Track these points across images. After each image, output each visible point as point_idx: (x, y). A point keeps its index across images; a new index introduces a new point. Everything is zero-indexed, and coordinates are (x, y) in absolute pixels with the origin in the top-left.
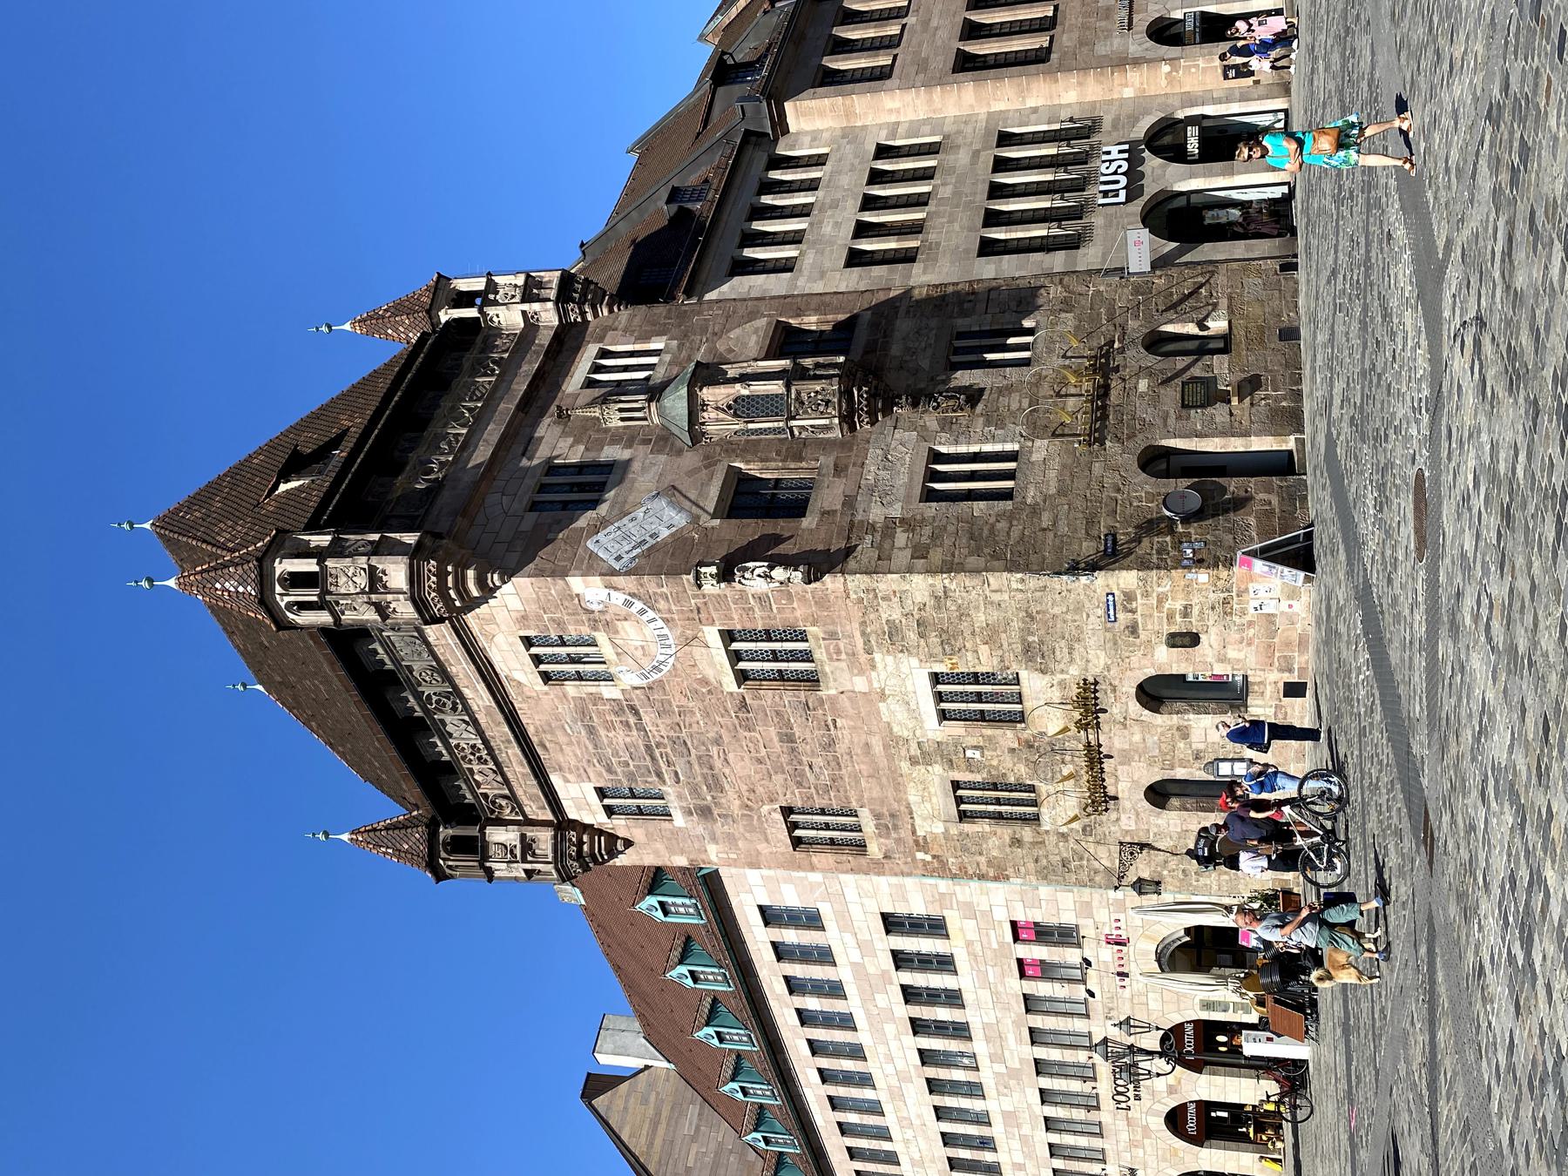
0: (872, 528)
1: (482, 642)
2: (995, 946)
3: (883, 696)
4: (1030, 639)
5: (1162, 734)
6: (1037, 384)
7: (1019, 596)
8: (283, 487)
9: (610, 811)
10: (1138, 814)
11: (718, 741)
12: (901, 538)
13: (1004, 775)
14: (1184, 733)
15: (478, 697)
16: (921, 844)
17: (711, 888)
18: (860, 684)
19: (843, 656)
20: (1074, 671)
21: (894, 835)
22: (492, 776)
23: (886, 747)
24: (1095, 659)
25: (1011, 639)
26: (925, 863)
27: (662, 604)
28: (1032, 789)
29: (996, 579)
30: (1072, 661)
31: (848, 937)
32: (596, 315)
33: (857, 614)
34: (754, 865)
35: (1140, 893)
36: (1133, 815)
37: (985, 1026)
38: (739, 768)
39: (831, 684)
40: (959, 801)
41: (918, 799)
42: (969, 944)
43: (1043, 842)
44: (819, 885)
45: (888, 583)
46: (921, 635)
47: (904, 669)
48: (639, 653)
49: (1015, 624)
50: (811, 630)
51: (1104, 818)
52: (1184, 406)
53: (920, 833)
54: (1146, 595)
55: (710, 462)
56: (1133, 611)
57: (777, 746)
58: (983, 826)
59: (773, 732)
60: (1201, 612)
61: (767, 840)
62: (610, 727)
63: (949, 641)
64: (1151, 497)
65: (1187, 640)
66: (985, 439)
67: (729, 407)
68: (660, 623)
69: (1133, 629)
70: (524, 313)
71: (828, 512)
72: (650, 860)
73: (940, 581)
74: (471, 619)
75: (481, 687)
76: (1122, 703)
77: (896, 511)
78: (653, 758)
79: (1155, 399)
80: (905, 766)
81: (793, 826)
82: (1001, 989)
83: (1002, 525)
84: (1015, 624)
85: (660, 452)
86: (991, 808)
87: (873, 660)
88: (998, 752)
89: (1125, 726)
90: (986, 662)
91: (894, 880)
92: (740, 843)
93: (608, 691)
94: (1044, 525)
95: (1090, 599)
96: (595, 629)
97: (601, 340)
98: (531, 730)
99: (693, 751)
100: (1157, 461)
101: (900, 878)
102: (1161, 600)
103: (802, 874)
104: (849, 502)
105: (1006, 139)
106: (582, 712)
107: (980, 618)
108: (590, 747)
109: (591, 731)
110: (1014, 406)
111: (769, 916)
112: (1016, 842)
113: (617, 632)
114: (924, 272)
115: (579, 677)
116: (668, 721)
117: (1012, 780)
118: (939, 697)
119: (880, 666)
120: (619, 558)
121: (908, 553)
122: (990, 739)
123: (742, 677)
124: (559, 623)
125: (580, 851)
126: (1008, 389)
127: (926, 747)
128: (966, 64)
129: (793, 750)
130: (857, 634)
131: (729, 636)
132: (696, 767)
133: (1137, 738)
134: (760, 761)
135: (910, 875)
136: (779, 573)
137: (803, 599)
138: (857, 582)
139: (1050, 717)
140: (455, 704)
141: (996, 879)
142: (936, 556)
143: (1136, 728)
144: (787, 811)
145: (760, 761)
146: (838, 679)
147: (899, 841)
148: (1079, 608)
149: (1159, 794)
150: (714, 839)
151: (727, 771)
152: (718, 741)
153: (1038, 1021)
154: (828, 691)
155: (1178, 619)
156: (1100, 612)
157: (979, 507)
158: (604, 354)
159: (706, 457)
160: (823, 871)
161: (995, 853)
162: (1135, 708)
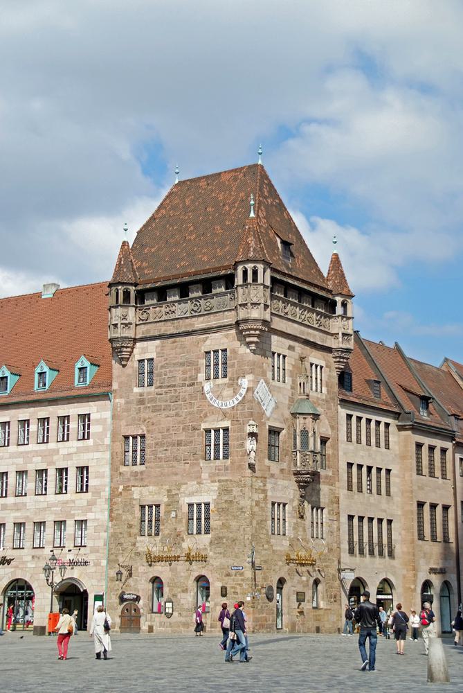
0: (265, 485)
1: (224, 333)
2: (72, 512)
3: (199, 483)
5: (184, 583)
6: (306, 541)
7: (242, 537)
8: (279, 241)
9: (141, 361)
10: (146, 573)
11: (177, 415)
12: (262, 496)
13: (164, 525)
14: (185, 591)
15: (199, 323)
17: (100, 394)
18: (205, 475)
20: (211, 554)
21: (132, 478)
22: (160, 315)
24: (216, 561)
25: (225, 533)
26: (117, 489)
28: (157, 534)
30: (215, 553)
31: (74, 450)
32: (335, 362)
33: (237, 478)
34: (114, 417)
35: (44, 569)
37: (24, 504)
38: (164, 420)
40: (150, 506)
41: (151, 491)
42: (73, 501)
43: (130, 536)
44: (103, 442)
47: (212, 493)
49: (231, 535)
51: (145, 560)
52: (297, 593)
54: (242, 580)
55: (285, 421)
56: (235, 575)
57: (175, 439)
58: (138, 514)
59: (183, 438)
61: (127, 425)
62: (184, 372)
63: (222, 511)
66: (290, 523)
67: (305, 428)
69: (228, 575)
70: (338, 334)
74: (233, 332)
75: (203, 326)
76: (197, 569)
77: (269, 493)
79: (300, 582)
80: (167, 487)
81: (135, 437)
82: (47, 512)
83: (265, 531)
84: (231, 535)
85: (289, 401)
86: (147, 518)
89: (188, 570)
92: (125, 413)
93: (201, 376)
95: (240, 561)
96: (230, 379)
97: (327, 367)
100: (281, 582)
103: (109, 435)
104: (272, 476)
105: (390, 522)
106: (190, 363)
107: (234, 523)
108: (174, 362)
109: (182, 364)
110: (299, 533)
111: (84, 417)
112: (130, 526)
113: (228, 387)
114: (344, 495)
115: (208, 366)
116: (187, 397)
117: (161, 527)
118: (199, 505)
119: (213, 484)
120: (258, 393)
122: (180, 521)
123: (208, 431)
124: (233, 365)
125: (124, 347)
126: (304, 530)
128: (421, 505)
129: (174, 445)
130: (226, 478)
131: (226, 430)
132: (165, 404)
133: (182, 574)
134: (168, 430)
135: (112, 482)
136: (253, 454)
137: (241, 461)
138: (248, 481)
139: (188, 544)
140: (195, 312)
142: (256, 509)
143: (186, 574)
144: (143, 436)
145: (168, 430)
146: (207, 468)
147: (129, 480)
148: (236, 557)
149: (156, 580)
150: (127, 403)
151: (163, 415)
152: (177, 415)
153: (29, 527)
154: (202, 463)
156: (235, 564)
157: (269, 522)
158: (321, 367)
159: (287, 419)
160: (112, 446)
161: (124, 517)
162: (196, 574)
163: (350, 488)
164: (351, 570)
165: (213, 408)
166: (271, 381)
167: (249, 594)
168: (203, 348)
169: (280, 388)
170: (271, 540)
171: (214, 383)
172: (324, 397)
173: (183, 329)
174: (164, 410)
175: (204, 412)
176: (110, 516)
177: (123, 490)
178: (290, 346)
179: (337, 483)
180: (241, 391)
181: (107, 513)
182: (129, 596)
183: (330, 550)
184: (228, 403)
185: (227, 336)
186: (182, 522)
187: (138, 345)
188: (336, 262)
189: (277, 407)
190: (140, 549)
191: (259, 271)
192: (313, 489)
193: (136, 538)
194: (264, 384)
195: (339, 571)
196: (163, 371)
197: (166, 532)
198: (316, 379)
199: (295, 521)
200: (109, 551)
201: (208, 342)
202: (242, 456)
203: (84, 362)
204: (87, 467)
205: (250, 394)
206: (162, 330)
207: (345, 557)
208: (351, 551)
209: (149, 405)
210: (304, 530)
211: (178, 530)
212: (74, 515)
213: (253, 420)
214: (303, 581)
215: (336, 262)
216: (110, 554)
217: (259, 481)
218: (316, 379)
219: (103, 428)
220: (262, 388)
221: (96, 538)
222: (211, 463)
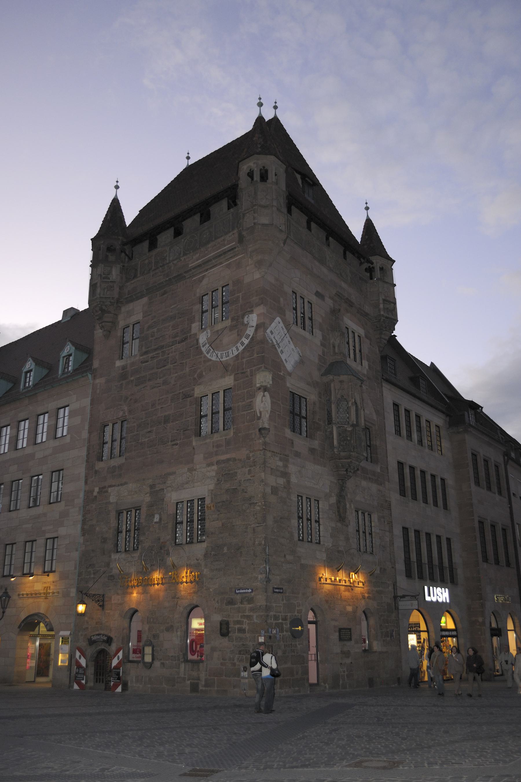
0: (286, 466)
2: (43, 529)
3: (191, 470)
4: (225, 550)
11: (165, 383)
12: (281, 481)
14: (170, 629)
16: (103, 490)
18: (199, 458)
19: (215, 449)
40: (128, 511)
46: (227, 491)
52: (340, 630)
53: (110, 490)
54: (252, 610)
58: (113, 523)
68: (236, 353)
69: (231, 602)
71: (293, 443)
72: (97, 348)
77: (294, 479)
78: (155, 350)
87: (213, 465)
90: (211, 525)
91: (83, 475)
94: (287, 557)
96: (233, 319)
99: (160, 370)
101: (84, 479)
102: (249, 617)
103: (87, 427)
104: (297, 454)
112: (104, 540)
113: (231, 330)
119: (209, 469)
120: (272, 332)
121: (274, 484)
130: (227, 456)
134: (153, 405)
141: (83, 529)
145: (153, 405)
152: (165, 383)
155: (237, 626)
156: (241, 585)
163: (403, 493)
164: (412, 596)
167: (263, 632)
168: (198, 291)
172: (365, 373)
175: (199, 371)
177: (98, 493)
178: (317, 292)
180: (248, 332)
181: (79, 526)
183: (383, 570)
184: (230, 351)
185: (228, 266)
189: (301, 362)
193: (110, 556)
194: (282, 325)
195: (395, 597)
198: (354, 347)
200: (79, 576)
201: (205, 282)
203: (69, 349)
205: (260, 333)
207: (402, 582)
209: (132, 378)
211: (161, 541)
217: (277, 459)
218: (354, 347)
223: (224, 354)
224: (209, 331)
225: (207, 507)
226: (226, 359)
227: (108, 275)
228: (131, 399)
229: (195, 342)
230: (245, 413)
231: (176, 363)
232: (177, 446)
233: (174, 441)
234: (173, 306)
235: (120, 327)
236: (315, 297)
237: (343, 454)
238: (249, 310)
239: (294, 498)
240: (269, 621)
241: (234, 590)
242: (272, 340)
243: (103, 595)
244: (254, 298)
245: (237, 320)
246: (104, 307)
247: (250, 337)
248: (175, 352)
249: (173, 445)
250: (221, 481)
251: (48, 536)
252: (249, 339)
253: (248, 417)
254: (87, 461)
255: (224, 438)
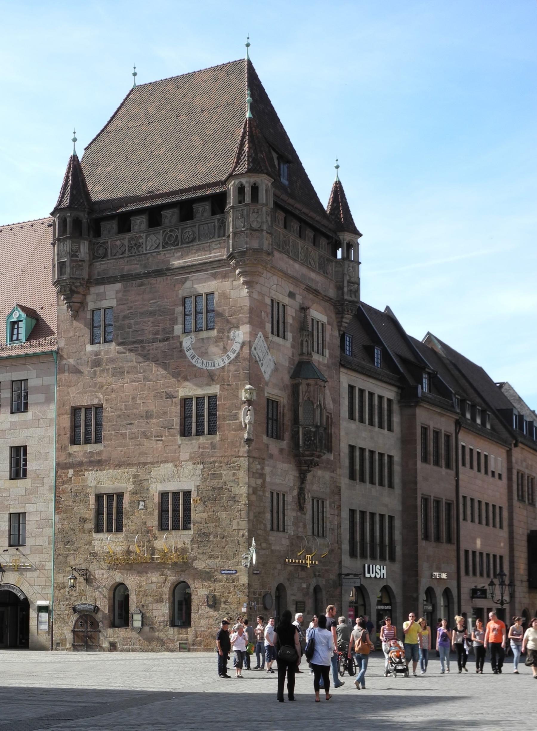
0: (263, 469)
3: (176, 466)
11: (146, 379)
12: (259, 482)
14: (160, 600)
18: (184, 455)
19: (201, 450)
23: (145, 464)
27: (233, 368)
29: (244, 524)
31: (8, 426)
36: (106, 577)
39: (184, 442)
40: (110, 496)
43: (84, 532)
45: (243, 475)
46: (214, 489)
48: (203, 350)
50: (217, 437)
57: (142, 409)
59: (152, 408)
60: (226, 609)
64: (270, 589)
65: (211, 603)
68: (222, 365)
71: (268, 447)
73: (244, 500)
77: (268, 479)
81: (88, 409)
83: (262, 526)
85: (290, 362)
86: (105, 510)
88: (142, 515)
93: (178, 329)
96: (218, 332)
98: (153, 281)
104: (271, 456)
106: (163, 312)
107: (223, 515)
109: (152, 314)
112: (84, 520)
117: (125, 521)
118: (176, 494)
120: (255, 349)
121: (254, 485)
122: (151, 514)
126: (305, 526)
127: (145, 484)
134: (133, 398)
142: (253, 498)
144: (99, 408)
145: (133, 398)
151: (126, 380)
154: (179, 440)
157: (268, 516)
165: (195, 369)
166: (270, 335)
167: (245, 604)
168: (180, 292)
169: (279, 345)
170: (270, 538)
171: (196, 337)
173: (154, 268)
174: (128, 372)
176: (57, 508)
177: (73, 475)
179: (338, 470)
181: (52, 505)
182: (84, 606)
184: (216, 362)
186: (153, 514)
187: (94, 290)
188: (338, 192)
189: (276, 370)
190: (96, 549)
191: (260, 189)
192: (314, 476)
193: (92, 536)
196: (127, 322)
197: (133, 528)
199: (295, 515)
200: (55, 550)
202: (235, 430)
204: (25, 448)
206: (126, 269)
208: (353, 554)
209: (107, 367)
210: (305, 526)
211: (148, 524)
212: (8, 507)
213: (250, 384)
214: (304, 588)
215: (338, 192)
216: (56, 557)
217: (257, 463)
219: (46, 398)
220: (260, 341)
221: (40, 534)
222: (190, 440)
223: (210, 364)
224: (193, 336)
225: (194, 500)
226: (212, 368)
227: (76, 252)
228: (107, 388)
229: (178, 344)
230: (231, 422)
231: (158, 361)
232: (162, 442)
233: (158, 436)
234: (151, 302)
235: (89, 309)
236: (287, 298)
237: (307, 453)
238: (235, 325)
239: (268, 495)
240: (250, 596)
241: (219, 571)
242: (255, 357)
243: (87, 570)
244: (240, 315)
245: (223, 333)
246: (73, 288)
247: (237, 352)
248: (156, 350)
249: (157, 440)
250: (207, 479)
251: (12, 511)
252: (235, 354)
253: (234, 427)
254: (57, 442)
255: (210, 441)
